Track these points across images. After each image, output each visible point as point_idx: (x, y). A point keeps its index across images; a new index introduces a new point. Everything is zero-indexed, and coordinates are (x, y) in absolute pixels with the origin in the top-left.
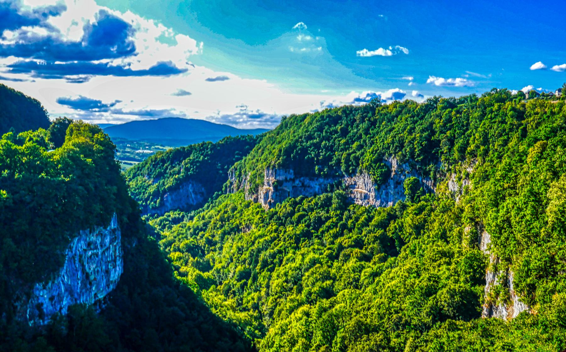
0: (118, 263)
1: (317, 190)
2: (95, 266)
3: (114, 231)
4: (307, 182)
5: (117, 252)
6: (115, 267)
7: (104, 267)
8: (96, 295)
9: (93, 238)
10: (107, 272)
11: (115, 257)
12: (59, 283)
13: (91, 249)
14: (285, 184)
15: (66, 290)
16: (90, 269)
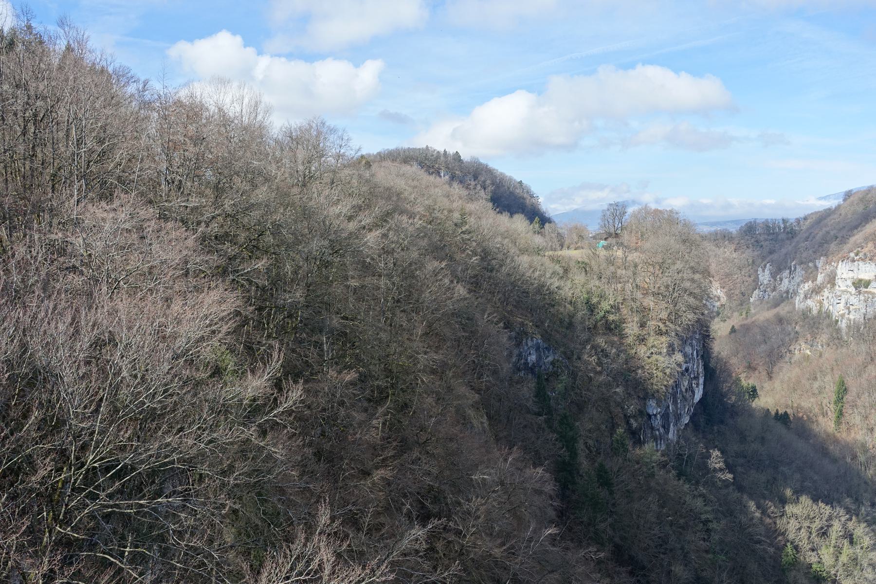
6: (698, 385)
11: (698, 374)
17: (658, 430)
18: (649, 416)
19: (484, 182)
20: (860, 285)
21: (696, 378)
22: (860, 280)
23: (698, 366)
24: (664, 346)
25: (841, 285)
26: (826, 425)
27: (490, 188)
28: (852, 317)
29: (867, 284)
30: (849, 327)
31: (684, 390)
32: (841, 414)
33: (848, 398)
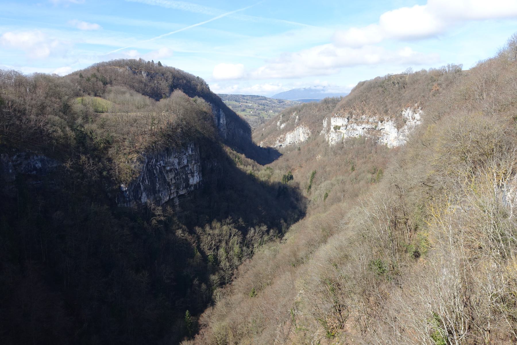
0: (196, 174)
1: (361, 132)
2: (173, 176)
3: (190, 156)
4: (355, 126)
5: (195, 167)
6: (193, 176)
7: (184, 177)
8: (177, 192)
9: (171, 160)
10: (187, 180)
12: (139, 184)
13: (168, 166)
14: (341, 128)
15: (145, 189)
16: (168, 177)
17: (129, 197)
18: (123, 192)
19: (167, 77)
20: (337, 128)
21: (192, 174)
22: (337, 126)
23: (193, 168)
24: (135, 158)
25: (332, 129)
26: (305, 193)
27: (170, 81)
28: (333, 143)
29: (339, 128)
30: (332, 148)
31: (167, 178)
32: (310, 187)
33: (314, 181)
